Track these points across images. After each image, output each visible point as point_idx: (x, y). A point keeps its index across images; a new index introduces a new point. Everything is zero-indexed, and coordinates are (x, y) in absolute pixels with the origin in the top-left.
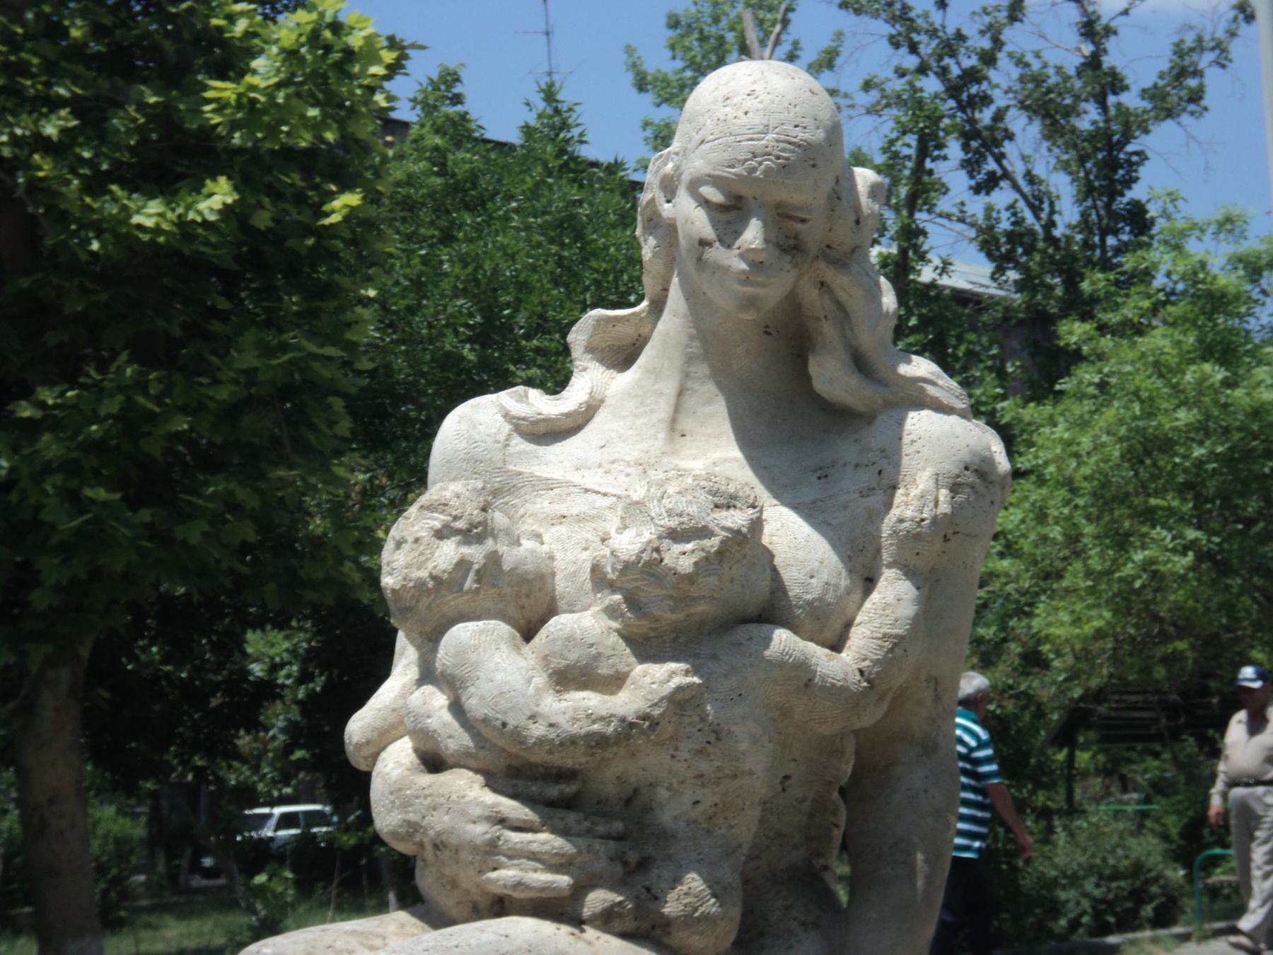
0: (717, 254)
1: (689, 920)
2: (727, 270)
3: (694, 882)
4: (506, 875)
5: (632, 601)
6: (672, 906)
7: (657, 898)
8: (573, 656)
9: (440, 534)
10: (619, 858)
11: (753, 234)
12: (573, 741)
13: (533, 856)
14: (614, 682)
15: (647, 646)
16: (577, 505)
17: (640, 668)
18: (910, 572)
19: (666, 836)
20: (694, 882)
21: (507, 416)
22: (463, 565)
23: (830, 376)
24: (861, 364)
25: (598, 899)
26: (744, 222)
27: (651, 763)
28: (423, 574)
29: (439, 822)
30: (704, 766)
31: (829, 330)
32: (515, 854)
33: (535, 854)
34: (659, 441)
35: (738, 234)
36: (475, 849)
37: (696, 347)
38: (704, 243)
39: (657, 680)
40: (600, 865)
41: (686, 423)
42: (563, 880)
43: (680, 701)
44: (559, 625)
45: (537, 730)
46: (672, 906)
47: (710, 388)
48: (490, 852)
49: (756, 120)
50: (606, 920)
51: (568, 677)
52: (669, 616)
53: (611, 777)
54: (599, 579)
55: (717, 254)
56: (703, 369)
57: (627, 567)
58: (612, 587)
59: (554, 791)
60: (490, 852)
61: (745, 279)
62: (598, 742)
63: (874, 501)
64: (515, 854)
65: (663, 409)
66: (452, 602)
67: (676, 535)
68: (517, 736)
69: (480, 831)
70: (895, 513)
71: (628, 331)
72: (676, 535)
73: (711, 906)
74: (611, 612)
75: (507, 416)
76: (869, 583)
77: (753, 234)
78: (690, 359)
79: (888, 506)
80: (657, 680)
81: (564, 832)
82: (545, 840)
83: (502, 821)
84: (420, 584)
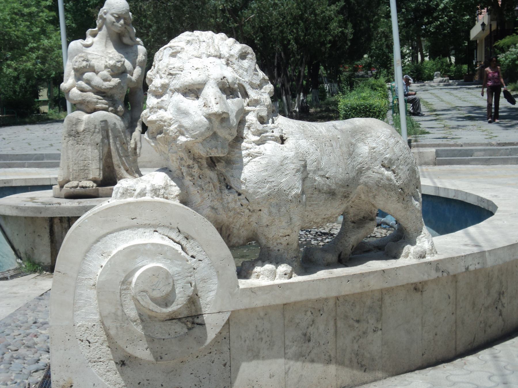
0: (116, 24)
1: (120, 111)
2: (118, 26)
3: (121, 106)
4: (99, 106)
5: (112, 70)
6: (118, 110)
7: (117, 108)
8: (105, 77)
9: (83, 60)
10: (112, 103)
11: (122, 22)
12: (108, 88)
13: (103, 103)
14: (110, 81)
15: (114, 76)
16: (95, 57)
17: (113, 79)
18: (140, 67)
19: (116, 101)
20: (121, 106)
21: (82, 44)
22: (87, 65)
23: (126, 40)
24: (131, 39)
25: (111, 109)
26: (121, 20)
27: (114, 91)
28: (82, 66)
29: (89, 99)
30: (121, 91)
31: (127, 34)
32: (100, 103)
33: (102, 103)
34: (104, 48)
35: (119, 21)
36: (94, 102)
37: (108, 36)
38: (114, 22)
39: (117, 80)
40: (111, 104)
41: (107, 46)
42: (107, 106)
43: (119, 83)
44: (101, 73)
45: (104, 87)
46: (118, 110)
47: (110, 41)
48: (97, 103)
49: (122, 6)
50: (112, 111)
51: (105, 80)
52: (116, 72)
53: (110, 93)
54: (106, 67)
55: (116, 24)
56: (109, 38)
57: (112, 66)
58: (109, 68)
59: (103, 95)
60: (97, 103)
61: (120, 27)
62: (111, 89)
63: (135, 57)
64: (100, 103)
65: (104, 44)
66: (85, 70)
67: (118, 62)
68: (101, 88)
69: (95, 100)
70: (138, 59)
71: (95, 32)
72: (118, 62)
73: (122, 109)
74: (109, 72)
75: (82, 44)
76: (134, 68)
77: (122, 22)
78: (107, 37)
79: (137, 58)
80: (115, 81)
81: (106, 100)
82: (104, 101)
83: (98, 99)
84: (81, 68)
